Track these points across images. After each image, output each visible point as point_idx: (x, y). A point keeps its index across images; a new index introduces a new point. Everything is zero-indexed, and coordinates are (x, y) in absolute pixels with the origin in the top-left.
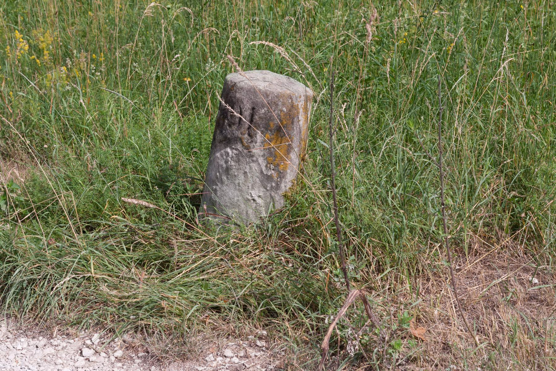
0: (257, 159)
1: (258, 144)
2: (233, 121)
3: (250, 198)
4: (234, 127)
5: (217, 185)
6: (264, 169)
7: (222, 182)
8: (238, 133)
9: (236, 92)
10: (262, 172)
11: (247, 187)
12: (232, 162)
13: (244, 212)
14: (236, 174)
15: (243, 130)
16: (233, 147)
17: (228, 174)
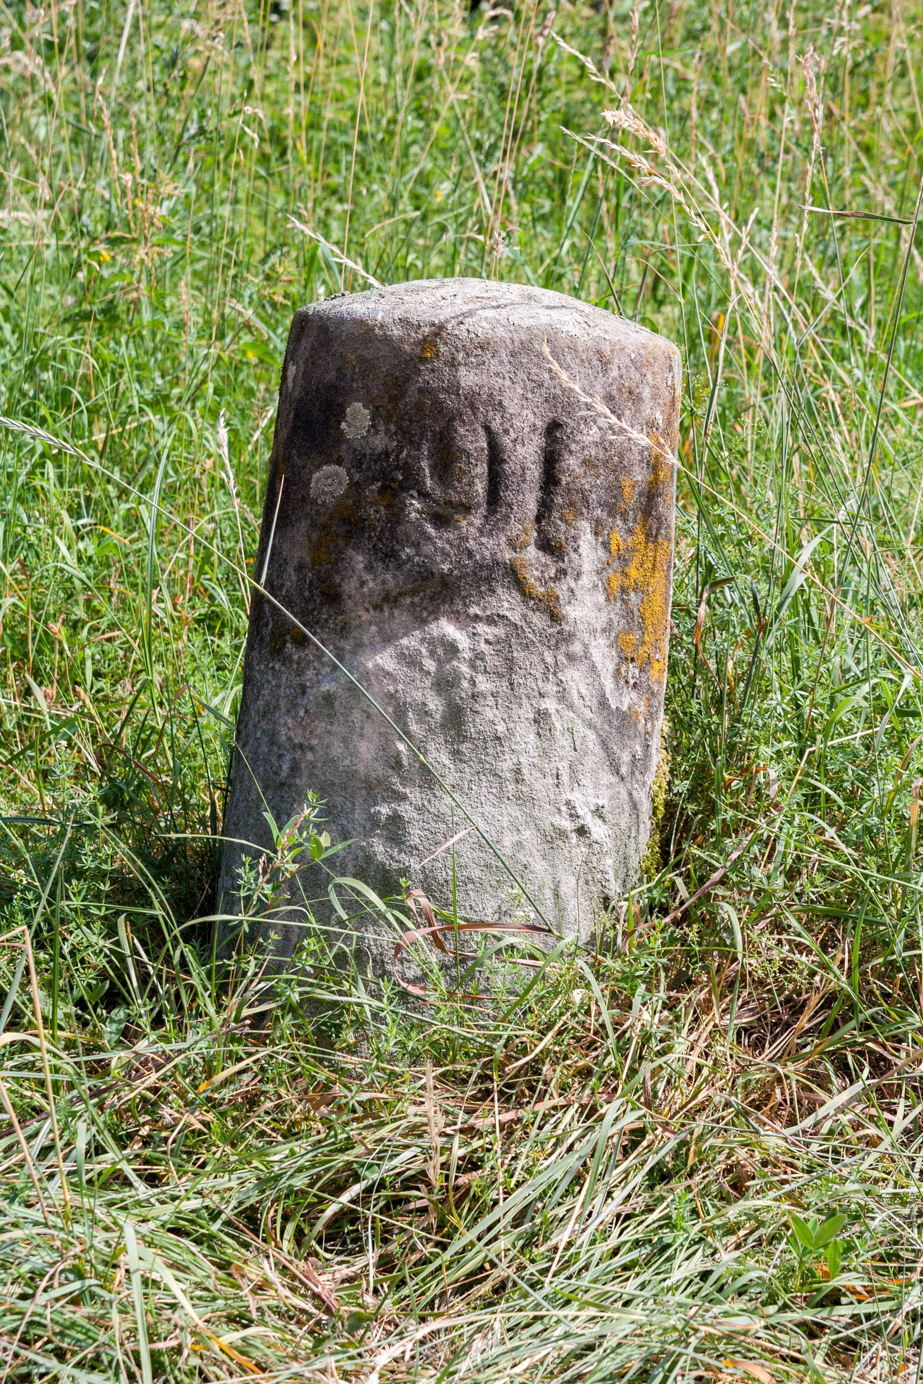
0: (586, 646)
1: (585, 580)
2: (455, 498)
3: (567, 825)
4: (470, 524)
5: (403, 798)
6: (609, 684)
7: (427, 778)
8: (495, 547)
9: (453, 364)
10: (603, 703)
11: (550, 781)
12: (480, 678)
13: (548, 893)
14: (501, 728)
15: (515, 528)
16: (474, 610)
17: (461, 737)
